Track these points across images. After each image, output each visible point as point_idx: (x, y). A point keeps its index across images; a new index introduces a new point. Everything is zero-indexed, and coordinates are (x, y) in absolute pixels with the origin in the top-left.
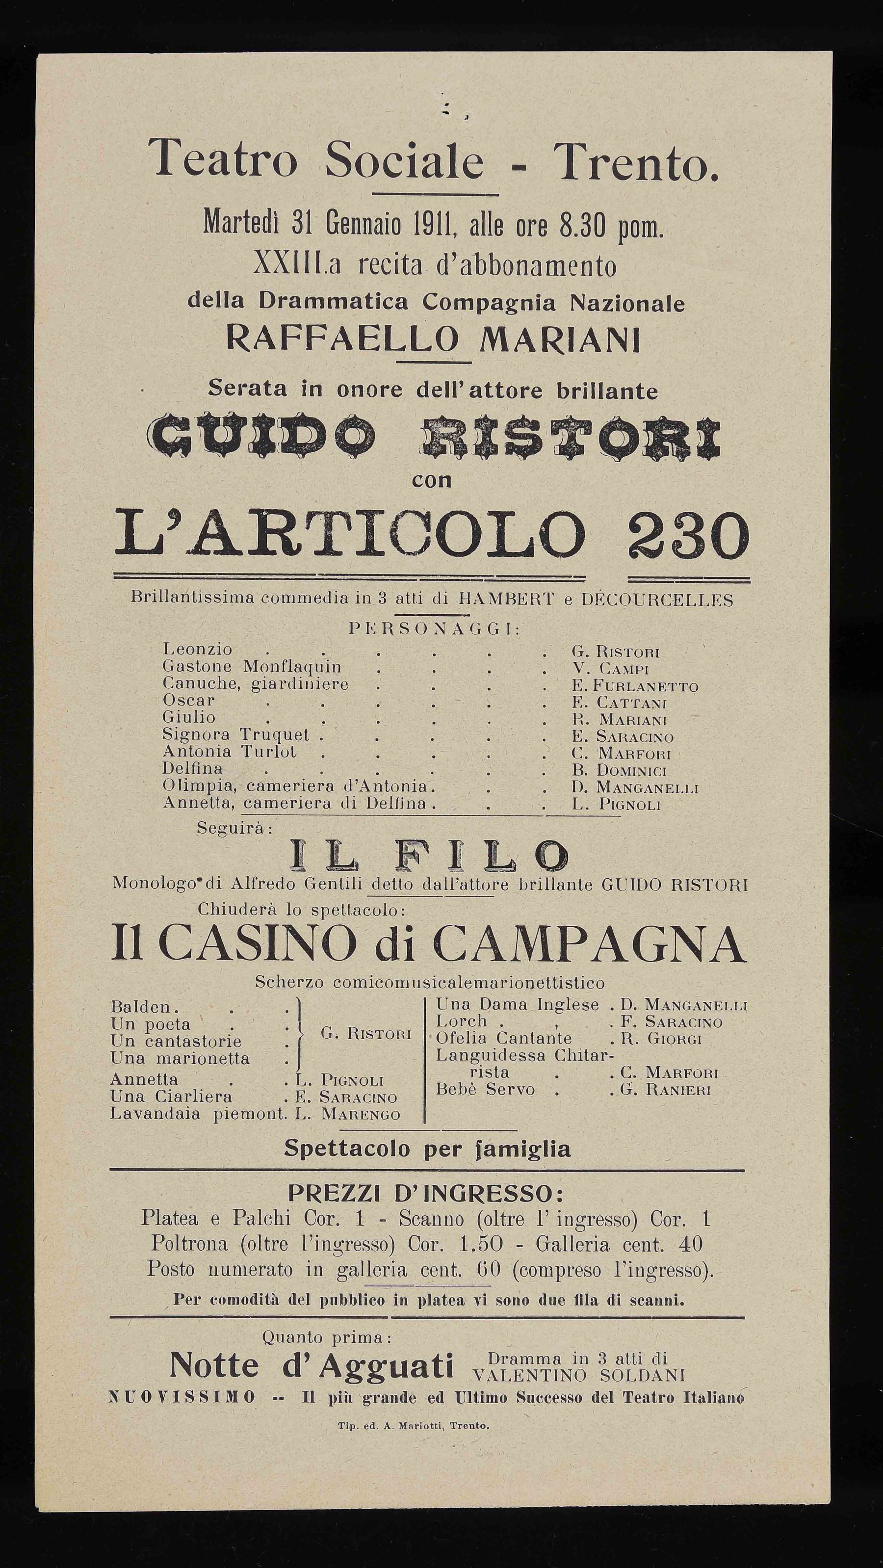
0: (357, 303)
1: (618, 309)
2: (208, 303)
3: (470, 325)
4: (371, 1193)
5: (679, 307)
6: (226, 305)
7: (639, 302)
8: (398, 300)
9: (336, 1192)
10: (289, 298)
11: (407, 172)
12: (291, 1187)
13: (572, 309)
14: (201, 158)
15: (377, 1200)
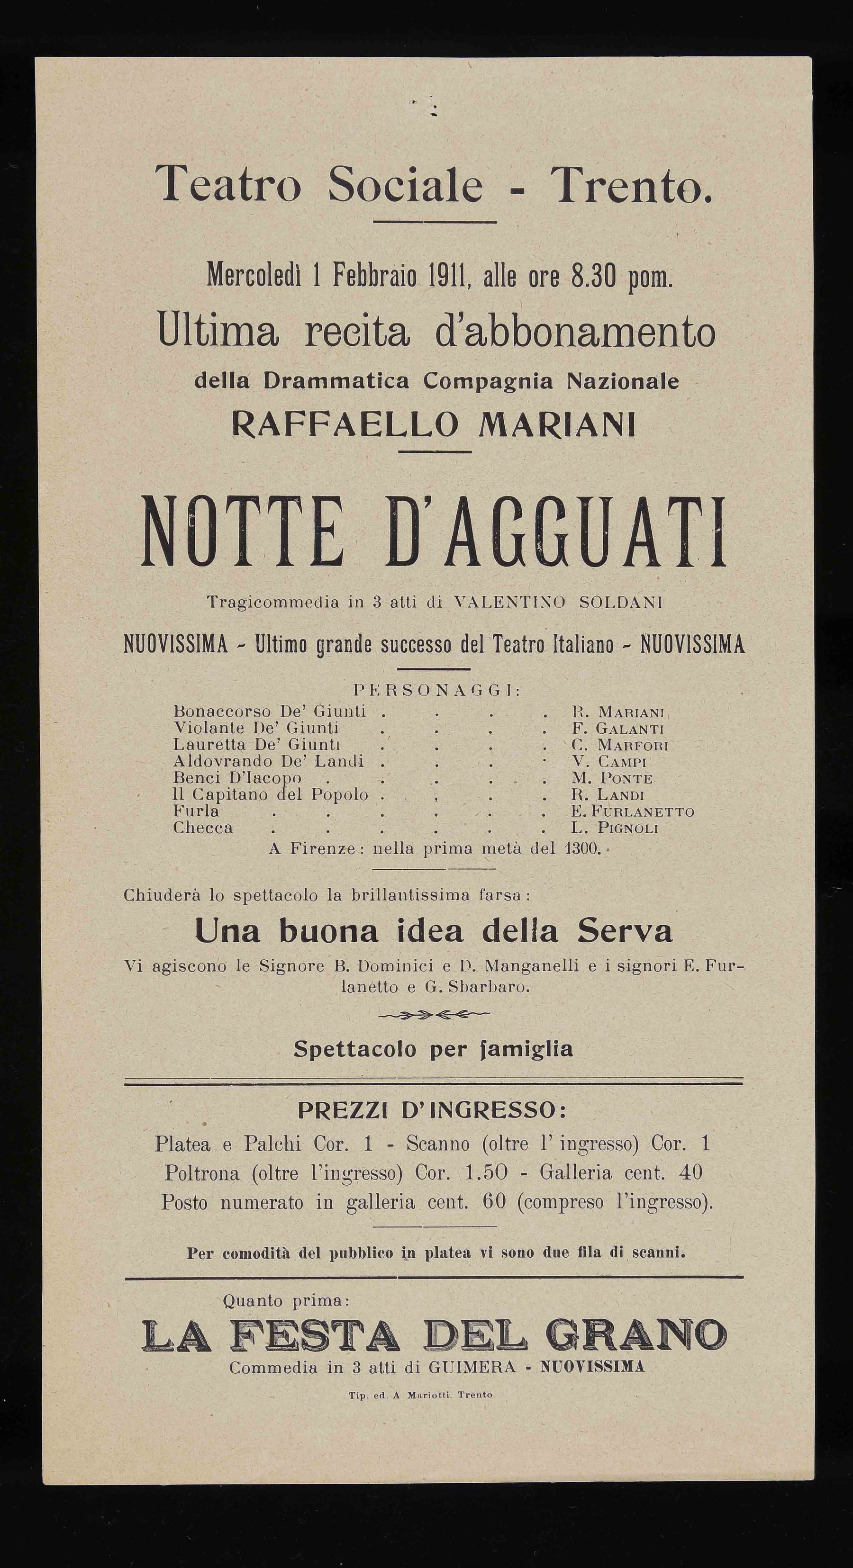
0: (359, 383)
1: (614, 387)
2: (215, 383)
3: (470, 406)
5: (673, 383)
6: (232, 386)
7: (634, 380)
8: (399, 379)
9: (345, 1109)
10: (293, 378)
11: (408, 196)
13: (569, 388)
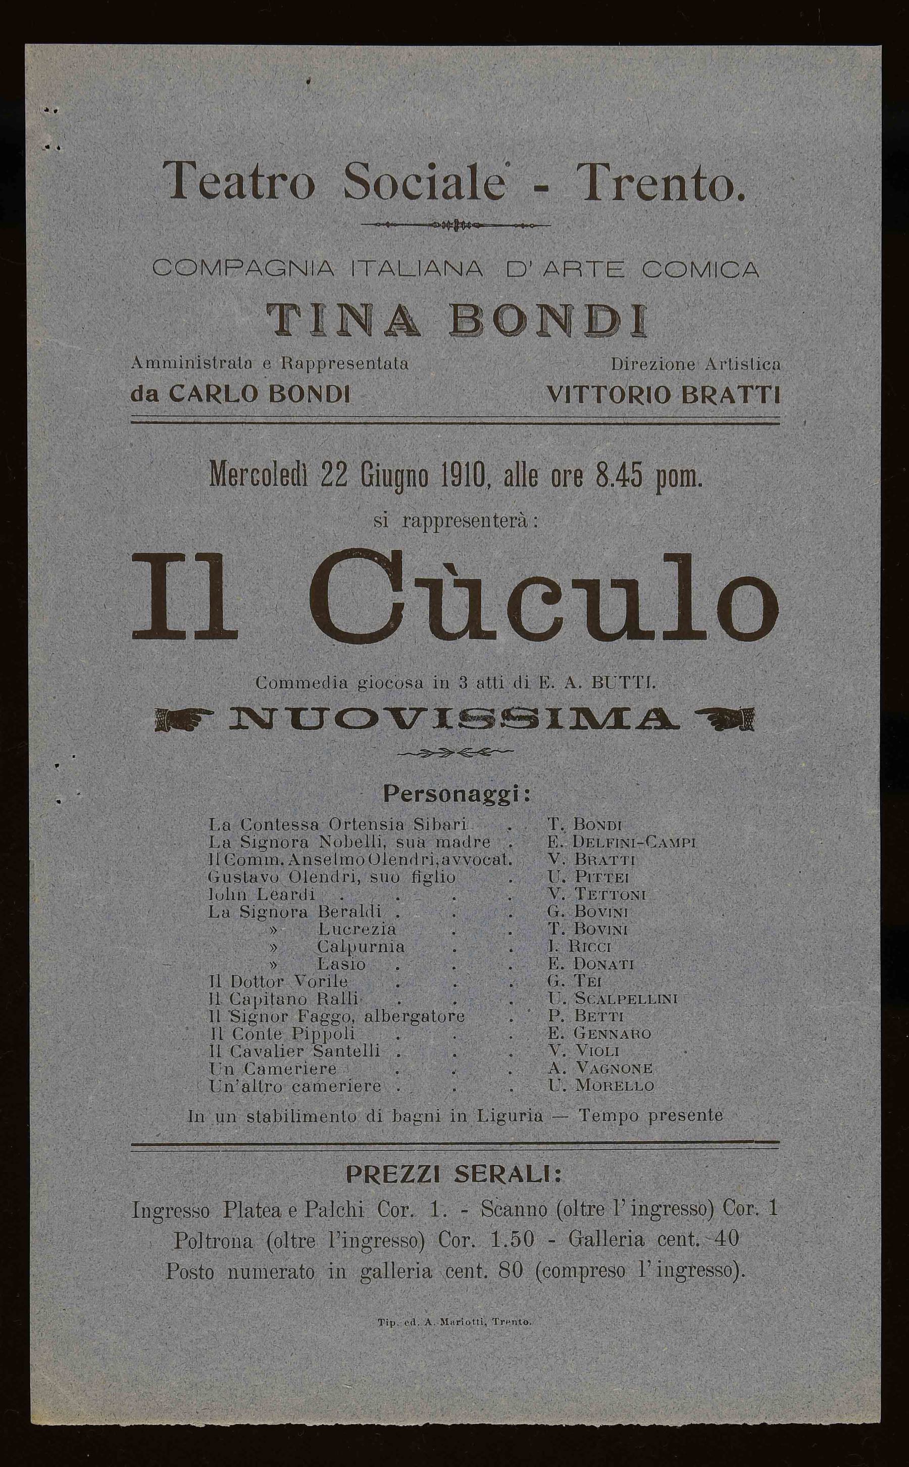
4: (431, 1174)
9: (395, 1173)
11: (427, 193)
12: (349, 1168)
14: (217, 181)
15: (437, 1180)
